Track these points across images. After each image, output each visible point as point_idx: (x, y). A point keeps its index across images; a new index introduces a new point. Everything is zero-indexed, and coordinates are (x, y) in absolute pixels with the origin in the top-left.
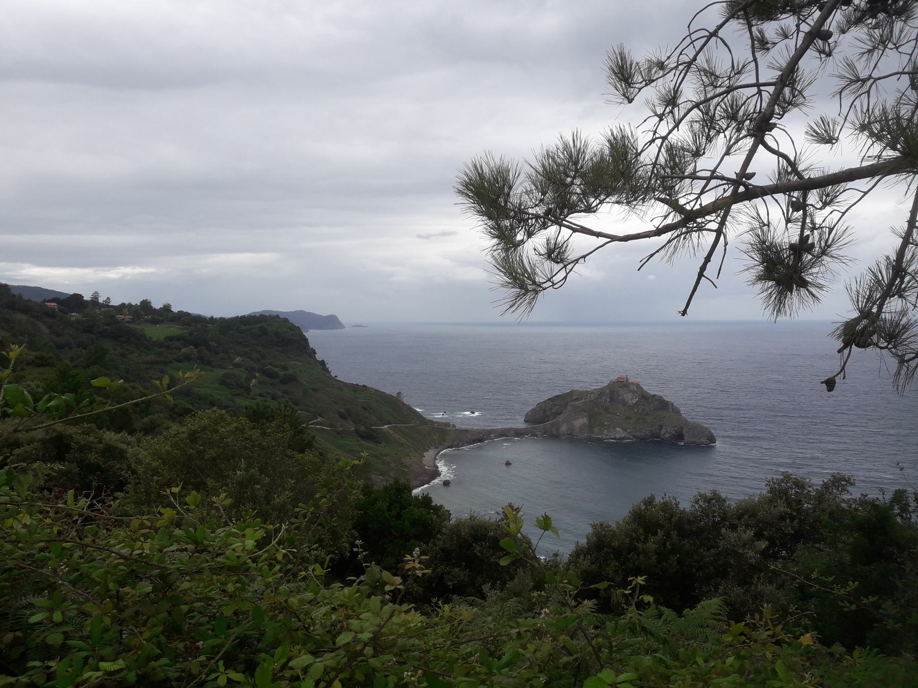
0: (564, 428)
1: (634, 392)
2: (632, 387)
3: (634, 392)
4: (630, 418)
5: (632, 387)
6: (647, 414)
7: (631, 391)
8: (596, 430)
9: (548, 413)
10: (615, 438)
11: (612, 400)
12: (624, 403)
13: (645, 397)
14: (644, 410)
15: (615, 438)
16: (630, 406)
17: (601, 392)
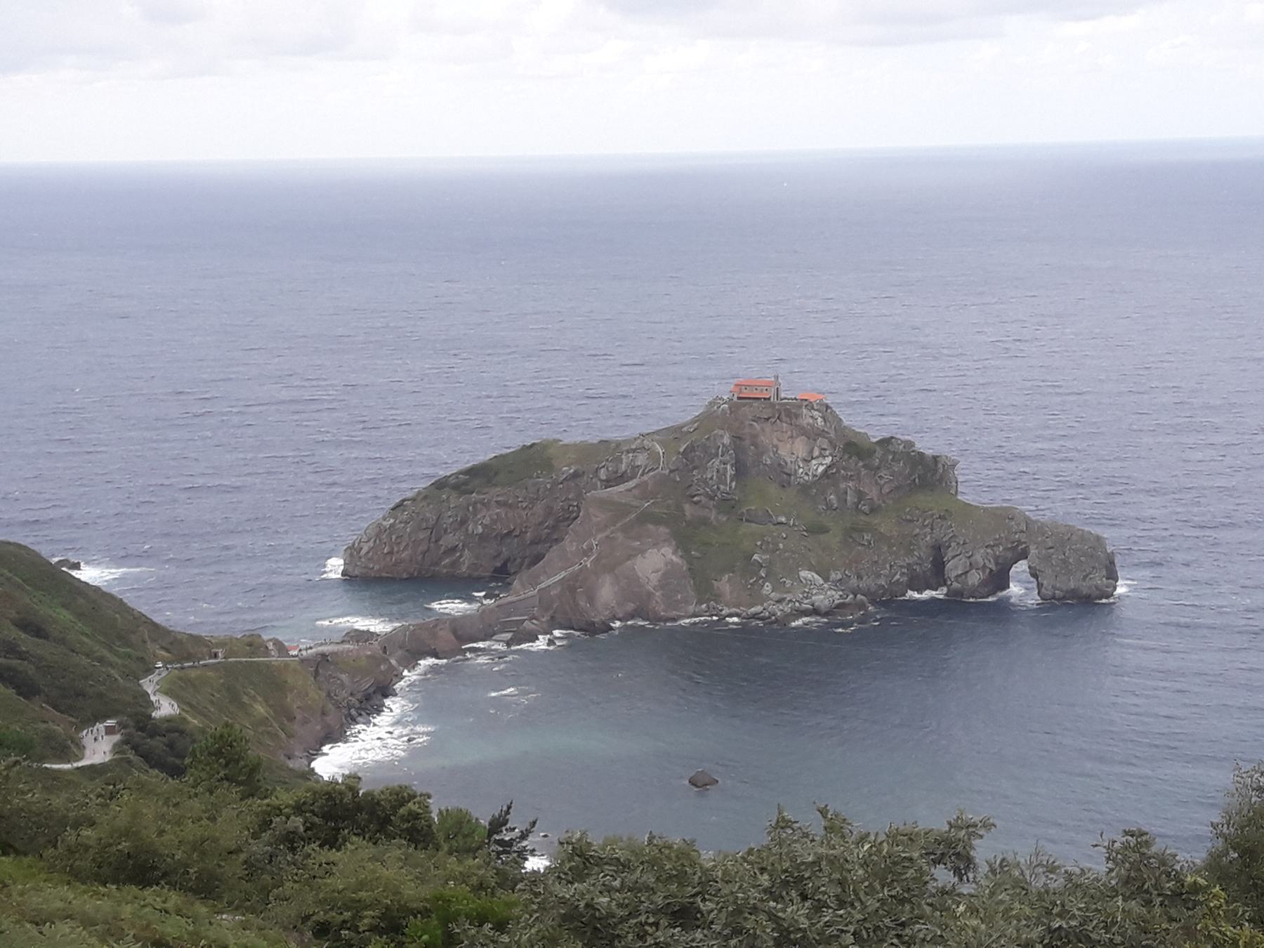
0: (607, 592)
1: (812, 435)
2: (806, 420)
3: (812, 435)
4: (823, 530)
5: (806, 420)
6: (874, 510)
7: (804, 432)
8: (724, 585)
9: (450, 540)
10: (815, 611)
11: (741, 471)
12: (782, 475)
13: (854, 449)
14: (860, 495)
15: (815, 611)
16: (804, 488)
17: (688, 447)
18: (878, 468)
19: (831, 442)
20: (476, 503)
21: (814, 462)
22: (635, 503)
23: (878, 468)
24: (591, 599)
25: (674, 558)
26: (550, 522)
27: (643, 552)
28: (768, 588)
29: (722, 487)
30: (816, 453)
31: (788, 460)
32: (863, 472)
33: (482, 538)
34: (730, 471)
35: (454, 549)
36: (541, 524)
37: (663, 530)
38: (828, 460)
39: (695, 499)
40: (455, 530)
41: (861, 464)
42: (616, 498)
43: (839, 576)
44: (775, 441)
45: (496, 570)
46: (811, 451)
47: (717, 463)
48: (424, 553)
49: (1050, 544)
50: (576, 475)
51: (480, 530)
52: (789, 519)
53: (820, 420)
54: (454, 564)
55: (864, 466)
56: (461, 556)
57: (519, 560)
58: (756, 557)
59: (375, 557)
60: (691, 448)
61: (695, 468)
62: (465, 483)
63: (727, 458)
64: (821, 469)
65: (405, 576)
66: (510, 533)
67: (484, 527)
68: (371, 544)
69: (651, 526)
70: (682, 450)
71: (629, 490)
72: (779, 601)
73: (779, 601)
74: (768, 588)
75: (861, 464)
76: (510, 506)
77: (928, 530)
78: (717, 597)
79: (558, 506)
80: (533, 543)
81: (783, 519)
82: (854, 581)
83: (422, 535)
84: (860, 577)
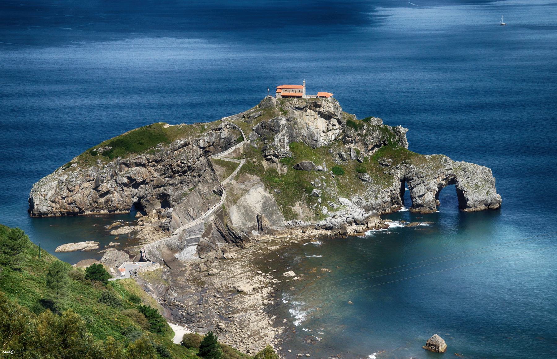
9: (104, 187)
18: (366, 135)
21: (330, 133)
22: (236, 161)
23: (366, 135)
24: (231, 222)
25: (265, 193)
26: (170, 173)
27: (247, 191)
28: (325, 210)
29: (282, 150)
30: (331, 126)
31: (315, 132)
32: (358, 137)
33: (126, 185)
35: (108, 192)
36: (163, 174)
37: (255, 178)
38: (337, 132)
39: (268, 157)
40: (108, 180)
41: (357, 133)
42: (225, 159)
43: (357, 200)
44: (307, 122)
45: (135, 204)
48: (87, 196)
49: (467, 176)
51: (125, 180)
52: (323, 168)
53: (332, 108)
54: (107, 202)
55: (359, 134)
56: (113, 197)
58: (315, 191)
59: (57, 200)
61: (265, 139)
62: (111, 151)
63: (284, 132)
65: (77, 210)
67: (129, 178)
68: (53, 192)
69: (249, 176)
70: (254, 128)
71: (229, 154)
72: (333, 217)
73: (333, 217)
74: (325, 210)
75: (357, 133)
76: (144, 165)
77: (399, 170)
78: (295, 216)
81: (320, 167)
82: (364, 203)
83: (87, 184)
84: (367, 199)
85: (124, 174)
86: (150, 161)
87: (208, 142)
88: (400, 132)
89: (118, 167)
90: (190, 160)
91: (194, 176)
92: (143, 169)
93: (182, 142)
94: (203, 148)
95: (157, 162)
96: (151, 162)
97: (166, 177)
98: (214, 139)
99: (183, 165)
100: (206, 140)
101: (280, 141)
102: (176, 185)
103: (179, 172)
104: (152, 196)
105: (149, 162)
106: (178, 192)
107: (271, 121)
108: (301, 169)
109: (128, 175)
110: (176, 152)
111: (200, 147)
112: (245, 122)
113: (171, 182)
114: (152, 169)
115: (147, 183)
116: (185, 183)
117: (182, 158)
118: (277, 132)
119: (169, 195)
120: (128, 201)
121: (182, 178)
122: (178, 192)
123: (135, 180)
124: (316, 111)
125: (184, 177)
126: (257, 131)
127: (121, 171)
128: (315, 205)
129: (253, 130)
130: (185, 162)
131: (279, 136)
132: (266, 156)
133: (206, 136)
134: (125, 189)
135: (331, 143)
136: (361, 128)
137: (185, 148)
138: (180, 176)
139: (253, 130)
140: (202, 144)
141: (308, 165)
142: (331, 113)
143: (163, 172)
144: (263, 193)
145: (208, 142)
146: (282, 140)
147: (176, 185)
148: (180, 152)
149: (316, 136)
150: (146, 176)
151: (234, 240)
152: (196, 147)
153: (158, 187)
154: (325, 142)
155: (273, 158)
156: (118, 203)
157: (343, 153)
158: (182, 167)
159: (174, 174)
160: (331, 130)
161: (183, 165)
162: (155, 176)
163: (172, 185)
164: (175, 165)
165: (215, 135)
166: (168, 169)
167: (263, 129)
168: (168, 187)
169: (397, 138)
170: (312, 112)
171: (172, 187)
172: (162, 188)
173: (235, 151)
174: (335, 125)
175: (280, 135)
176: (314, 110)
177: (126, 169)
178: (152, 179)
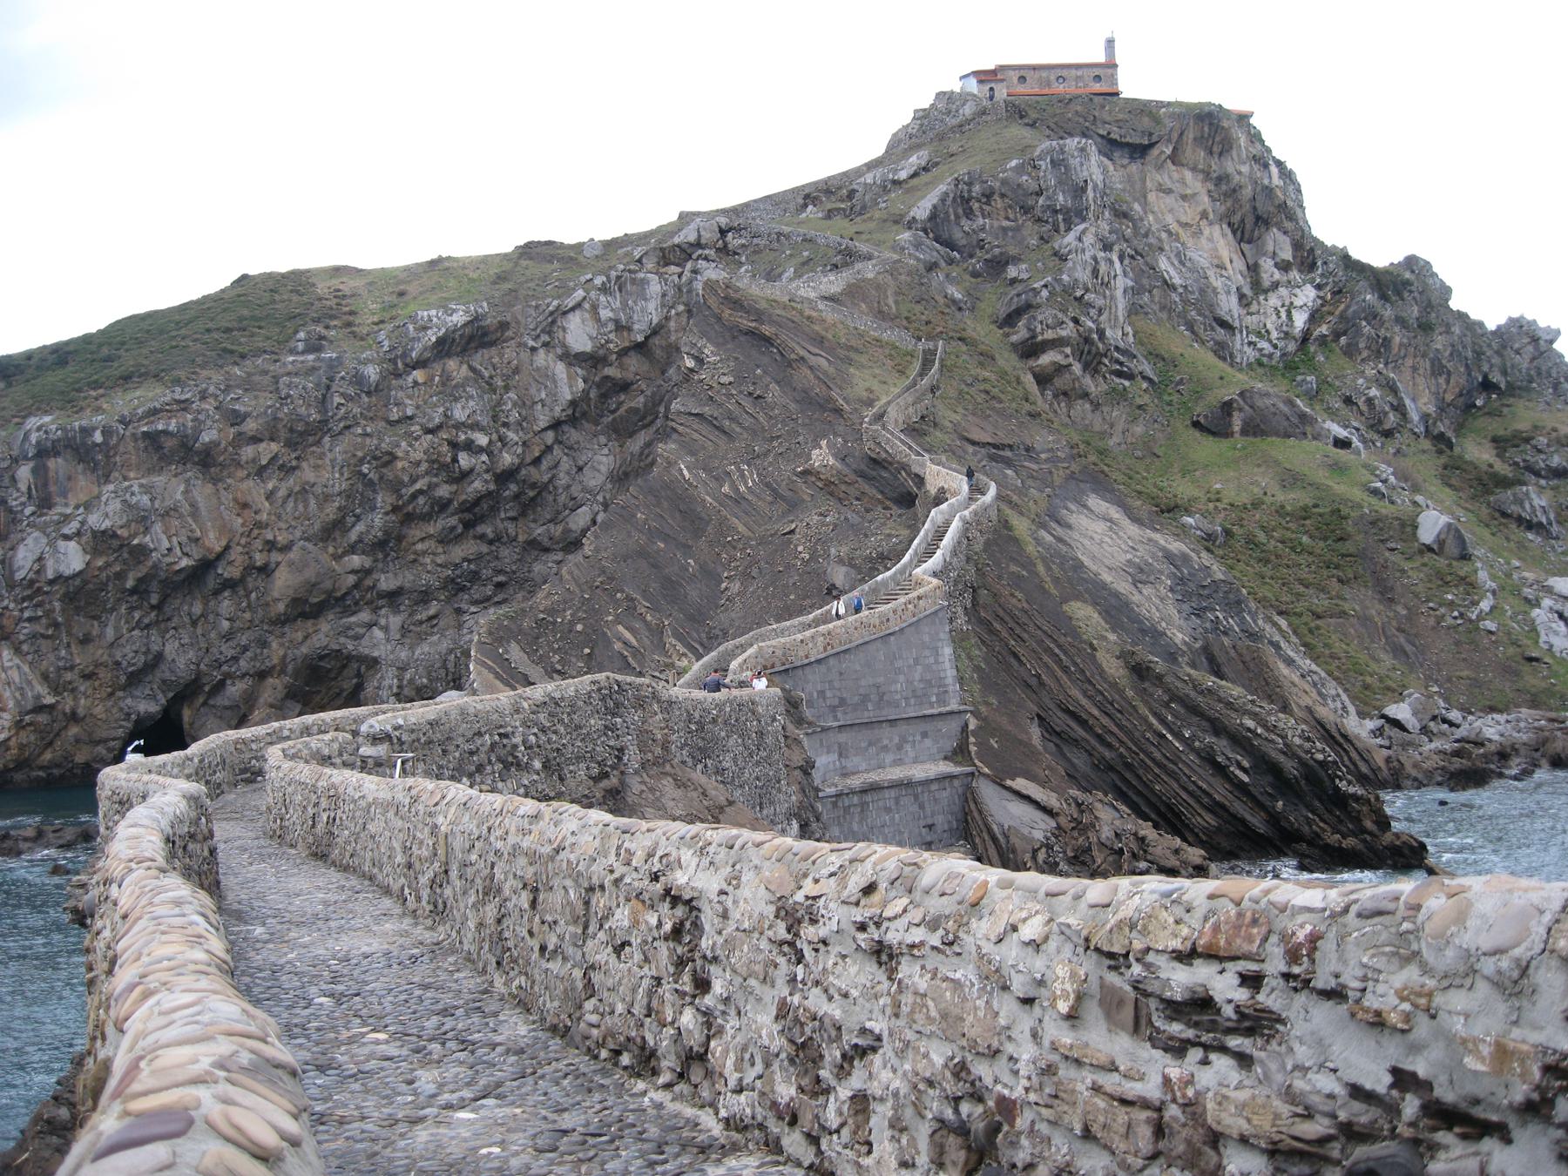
19: (1297, 246)
20: (43, 453)
26: (376, 522)
31: (1218, 283)
33: (81, 595)
34: (1121, 283)
38: (1307, 295)
39: (1046, 359)
44: (1174, 227)
46: (1253, 269)
47: (1089, 239)
50: (474, 338)
51: (73, 558)
55: (1401, 321)
57: (235, 690)
60: (963, 202)
61: (997, 265)
64: (1300, 320)
66: (206, 566)
70: (922, 210)
76: (206, 461)
79: (413, 451)
80: (305, 609)
85: (66, 518)
86: (250, 426)
87: (620, 327)
88: (1535, 340)
89: (24, 473)
90: (511, 435)
91: (533, 544)
92: (203, 492)
93: (459, 318)
94: (592, 360)
95: (302, 437)
96: (255, 440)
97: (352, 549)
98: (648, 312)
99: (464, 460)
100: (605, 314)
101: (1095, 273)
102: (425, 597)
103: (443, 506)
104: (262, 675)
105: (241, 440)
106: (432, 648)
107: (1020, 169)
108: (1251, 429)
109: (95, 520)
110: (418, 375)
111: (572, 359)
112: (829, 215)
113: (386, 582)
114: (254, 491)
115: (230, 584)
116: (477, 592)
117: (459, 414)
118: (1074, 214)
119: (373, 663)
120: (98, 710)
121: (458, 552)
122: (432, 648)
123: (141, 552)
124: (1207, 175)
125: (469, 548)
126: (935, 226)
127: (45, 503)
128: (1485, 605)
129: (911, 224)
130: (482, 440)
131: (1081, 242)
132: (1030, 349)
133: (604, 289)
134: (81, 625)
135: (1292, 347)
136: (1399, 294)
137: (478, 359)
138: (448, 539)
139: (911, 224)
140: (579, 334)
141: (1285, 409)
142: (1269, 191)
143: (331, 511)
144: (1133, 530)
145: (620, 327)
146: (1103, 268)
147: (425, 597)
148: (446, 378)
149: (1228, 305)
150: (224, 528)
151: (1257, 821)
152: (541, 358)
153: (305, 609)
154: (1264, 345)
155: (1077, 368)
156: (19, 725)
157: (1374, 392)
158: (465, 475)
159: (409, 519)
160: (1275, 286)
161: (464, 460)
162: (281, 539)
163: (393, 597)
164: (413, 451)
165: (655, 287)
166: (371, 483)
167: (969, 214)
168: (365, 616)
169: (1523, 362)
170: (1188, 175)
171: (395, 621)
172: (323, 635)
173: (854, 293)
174: (1284, 267)
175: (1089, 239)
176: (1194, 169)
177: (84, 485)
178: (259, 559)
